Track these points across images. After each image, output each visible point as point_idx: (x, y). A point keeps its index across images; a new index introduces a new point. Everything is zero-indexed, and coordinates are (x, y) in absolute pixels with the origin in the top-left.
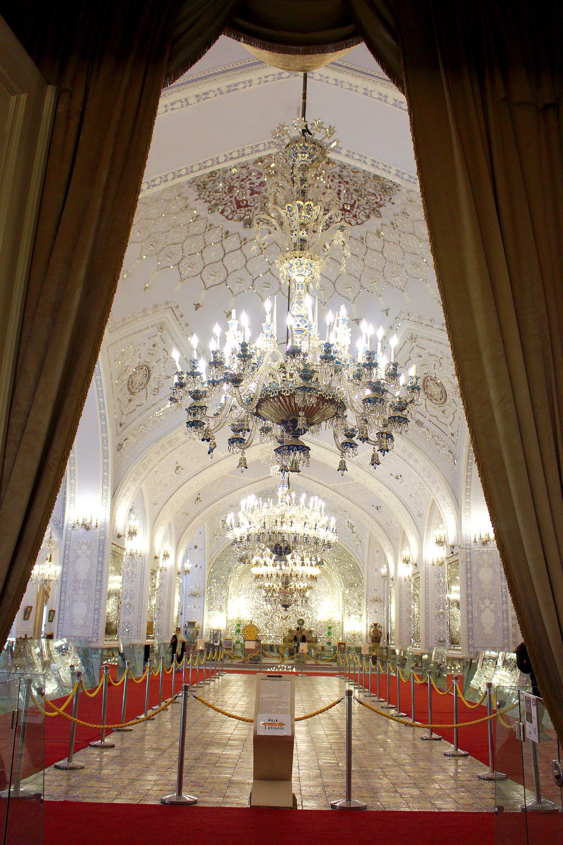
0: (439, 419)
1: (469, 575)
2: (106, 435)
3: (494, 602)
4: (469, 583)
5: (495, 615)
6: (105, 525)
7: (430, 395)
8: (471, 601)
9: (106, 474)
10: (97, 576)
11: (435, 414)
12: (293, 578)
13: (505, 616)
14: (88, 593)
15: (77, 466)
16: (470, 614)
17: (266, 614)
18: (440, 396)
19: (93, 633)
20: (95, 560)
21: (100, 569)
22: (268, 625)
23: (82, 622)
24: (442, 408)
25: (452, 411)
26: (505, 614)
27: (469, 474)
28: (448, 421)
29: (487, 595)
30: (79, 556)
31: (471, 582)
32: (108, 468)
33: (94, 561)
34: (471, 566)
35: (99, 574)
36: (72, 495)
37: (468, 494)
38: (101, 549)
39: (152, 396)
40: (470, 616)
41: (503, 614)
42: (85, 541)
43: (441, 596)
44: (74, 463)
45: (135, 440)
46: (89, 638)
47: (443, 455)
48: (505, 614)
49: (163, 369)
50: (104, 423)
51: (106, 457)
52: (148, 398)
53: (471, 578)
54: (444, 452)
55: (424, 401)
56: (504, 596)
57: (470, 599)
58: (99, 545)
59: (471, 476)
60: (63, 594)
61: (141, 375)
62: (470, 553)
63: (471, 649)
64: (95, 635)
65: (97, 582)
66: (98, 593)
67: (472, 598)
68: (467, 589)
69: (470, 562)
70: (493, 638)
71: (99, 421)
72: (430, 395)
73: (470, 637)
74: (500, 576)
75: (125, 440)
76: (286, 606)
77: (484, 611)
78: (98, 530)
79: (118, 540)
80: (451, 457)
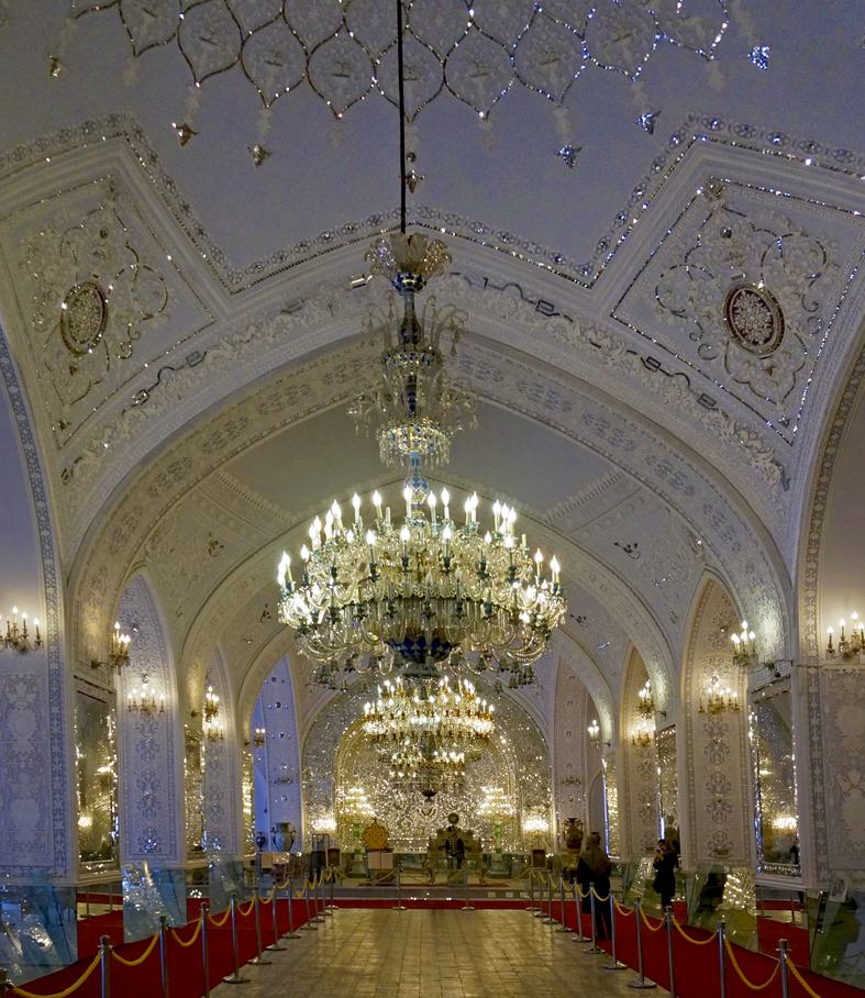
0: (756, 387)
1: (814, 721)
4: (815, 739)
6: (57, 641)
7: (741, 331)
8: (821, 774)
10: (53, 744)
11: (746, 378)
12: (444, 740)
14: (38, 778)
16: (819, 801)
17: (398, 808)
18: (766, 333)
19: (56, 859)
20: (45, 713)
21: (56, 730)
24: (766, 363)
27: (818, 508)
28: (776, 392)
29: (853, 762)
30: (12, 706)
33: (44, 715)
35: (56, 740)
37: (813, 551)
45: (99, 459)
46: (48, 868)
53: (819, 727)
55: (725, 348)
59: (822, 513)
62: (816, 676)
63: (824, 874)
64: (60, 862)
65: (53, 757)
66: (57, 778)
68: (812, 751)
69: (817, 694)
72: (741, 331)
73: (819, 849)
75: (76, 462)
76: (429, 794)
78: (44, 651)
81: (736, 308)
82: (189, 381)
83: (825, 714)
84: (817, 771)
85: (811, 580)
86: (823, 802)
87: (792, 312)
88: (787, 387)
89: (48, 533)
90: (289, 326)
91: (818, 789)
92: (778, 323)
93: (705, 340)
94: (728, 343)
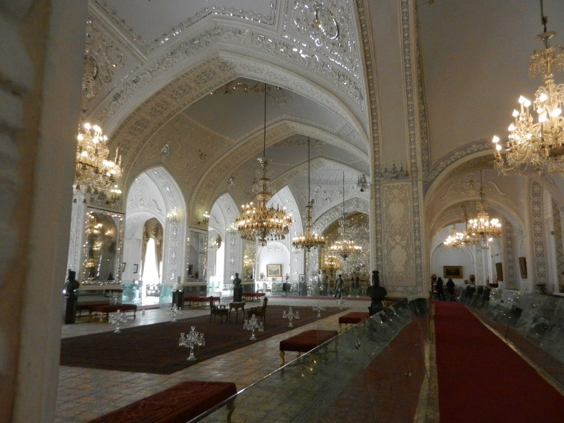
1: (378, 212)
3: (406, 238)
4: (378, 220)
5: (407, 252)
8: (381, 238)
13: (418, 252)
16: (379, 251)
26: (418, 251)
29: (397, 231)
31: (380, 219)
34: (380, 202)
39: (106, 84)
41: (416, 251)
47: (351, 94)
48: (418, 251)
49: (106, 58)
52: (103, 86)
53: (380, 215)
54: (351, 91)
56: (417, 232)
58: (78, 209)
61: (88, 65)
65: (76, 239)
66: (77, 247)
67: (381, 234)
68: (377, 226)
69: (380, 198)
70: (404, 276)
74: (412, 210)
77: (393, 248)
79: (107, 206)
82: (134, 88)
83: (383, 207)
84: (379, 236)
86: (381, 252)
91: (379, 245)
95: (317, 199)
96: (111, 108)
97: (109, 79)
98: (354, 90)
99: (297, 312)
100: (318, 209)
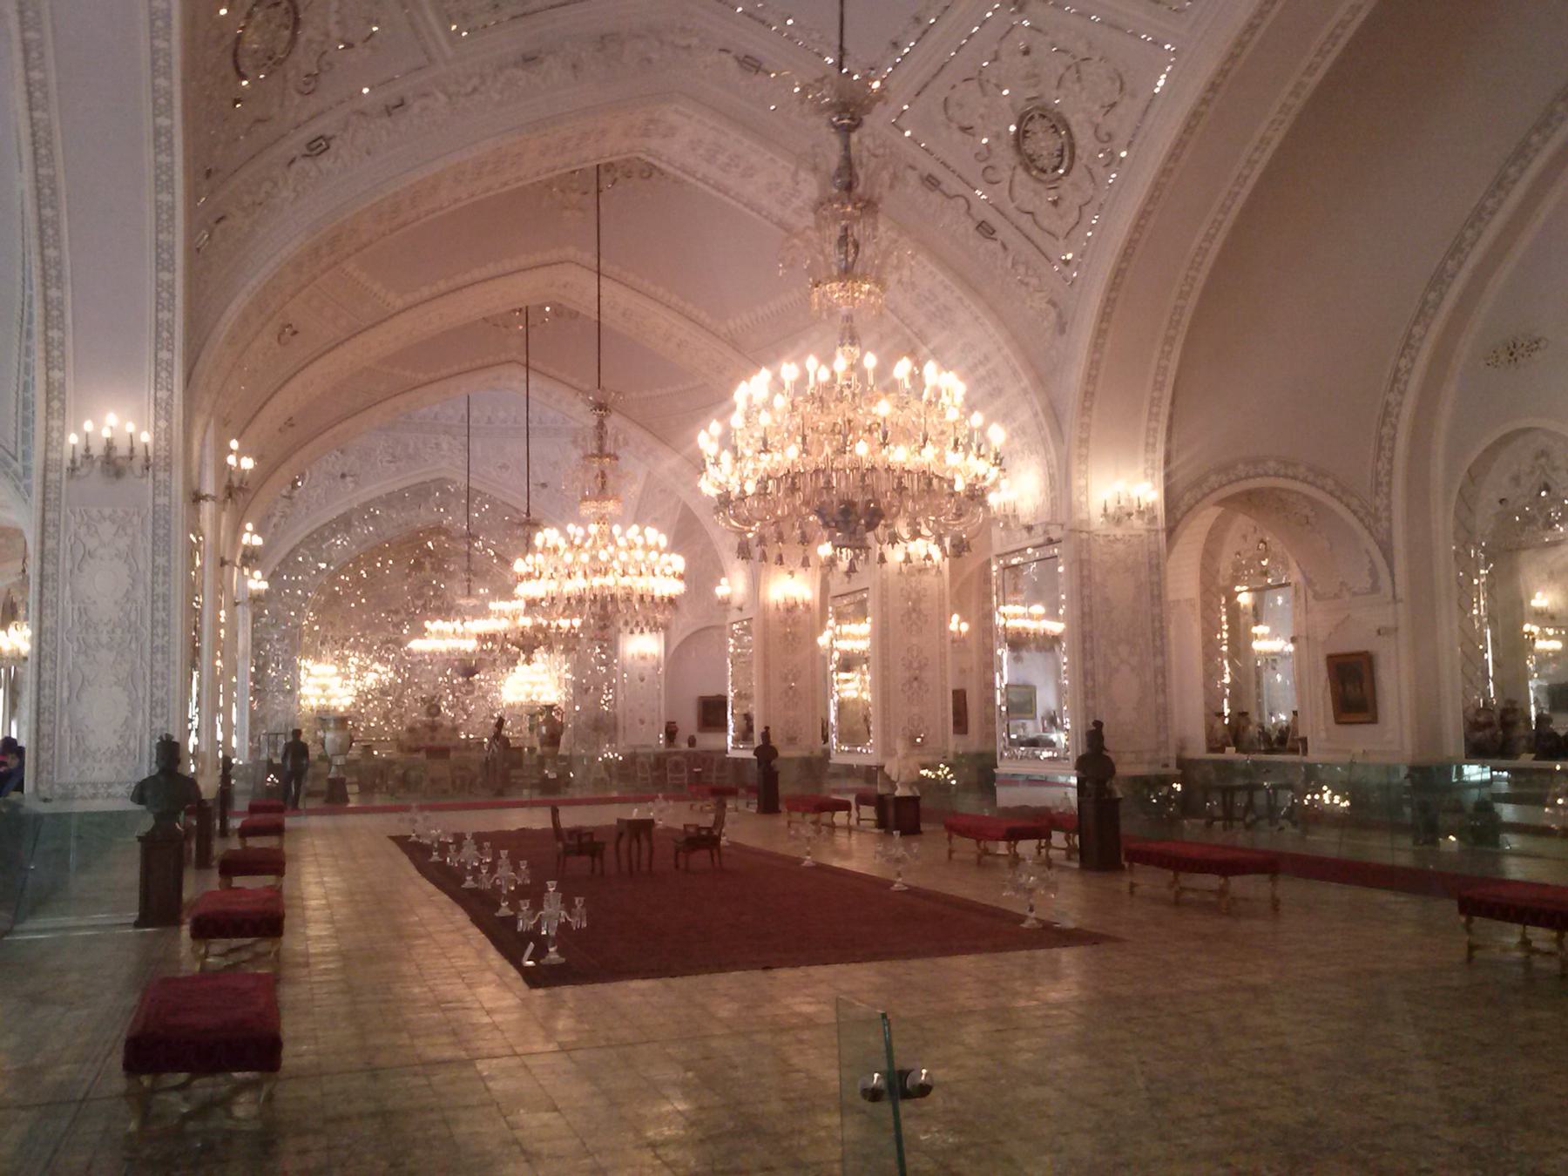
0: (1038, 218)
1: (1086, 592)
2: (160, 197)
9: (165, 315)
11: (1030, 208)
13: (1160, 680)
15: (68, 287)
18: (1056, 161)
21: (160, 590)
22: (391, 717)
23: (114, 742)
25: (1079, 201)
26: (1160, 677)
32: (173, 296)
33: (141, 566)
36: (56, 375)
38: (161, 532)
39: (298, 99)
40: (1090, 684)
41: (1156, 677)
42: (107, 511)
43: (914, 640)
44: (59, 277)
48: (1160, 677)
49: (334, 18)
50: (163, 158)
51: (163, 265)
53: (1090, 597)
56: (1158, 639)
57: (1088, 645)
60: (47, 664)
61: (273, 26)
65: (153, 627)
66: (159, 656)
71: (148, 151)
75: (218, 221)
80: (1053, 315)
81: (1027, 132)
85: (1084, 436)
87: (1084, 138)
88: (1072, 220)
89: (170, 315)
90: (520, 83)
92: (1068, 152)
93: (990, 162)
94: (1014, 168)
95: (311, 474)
96: (290, 181)
97: (311, 84)
98: (1044, 306)
99: (487, 844)
100: (308, 508)
